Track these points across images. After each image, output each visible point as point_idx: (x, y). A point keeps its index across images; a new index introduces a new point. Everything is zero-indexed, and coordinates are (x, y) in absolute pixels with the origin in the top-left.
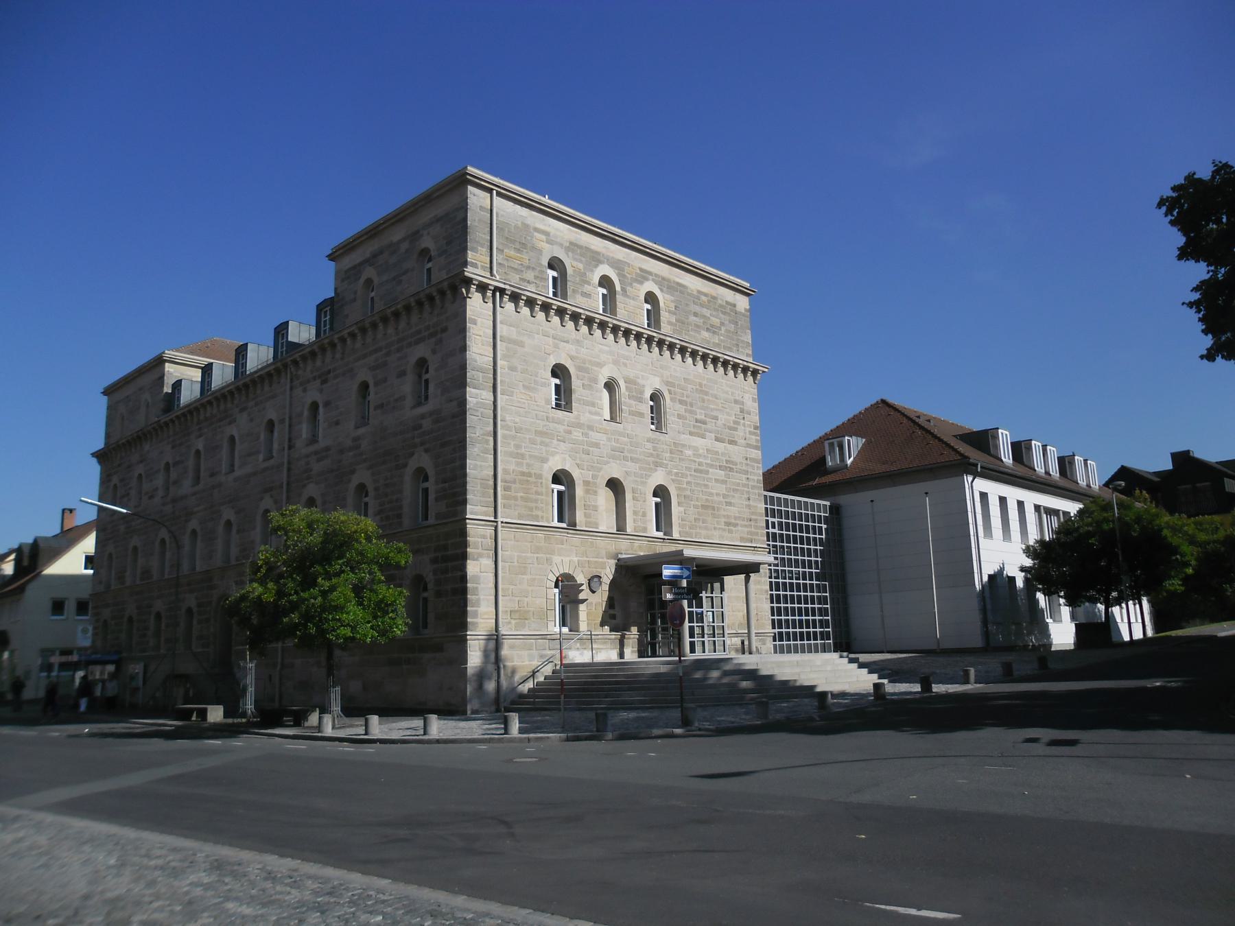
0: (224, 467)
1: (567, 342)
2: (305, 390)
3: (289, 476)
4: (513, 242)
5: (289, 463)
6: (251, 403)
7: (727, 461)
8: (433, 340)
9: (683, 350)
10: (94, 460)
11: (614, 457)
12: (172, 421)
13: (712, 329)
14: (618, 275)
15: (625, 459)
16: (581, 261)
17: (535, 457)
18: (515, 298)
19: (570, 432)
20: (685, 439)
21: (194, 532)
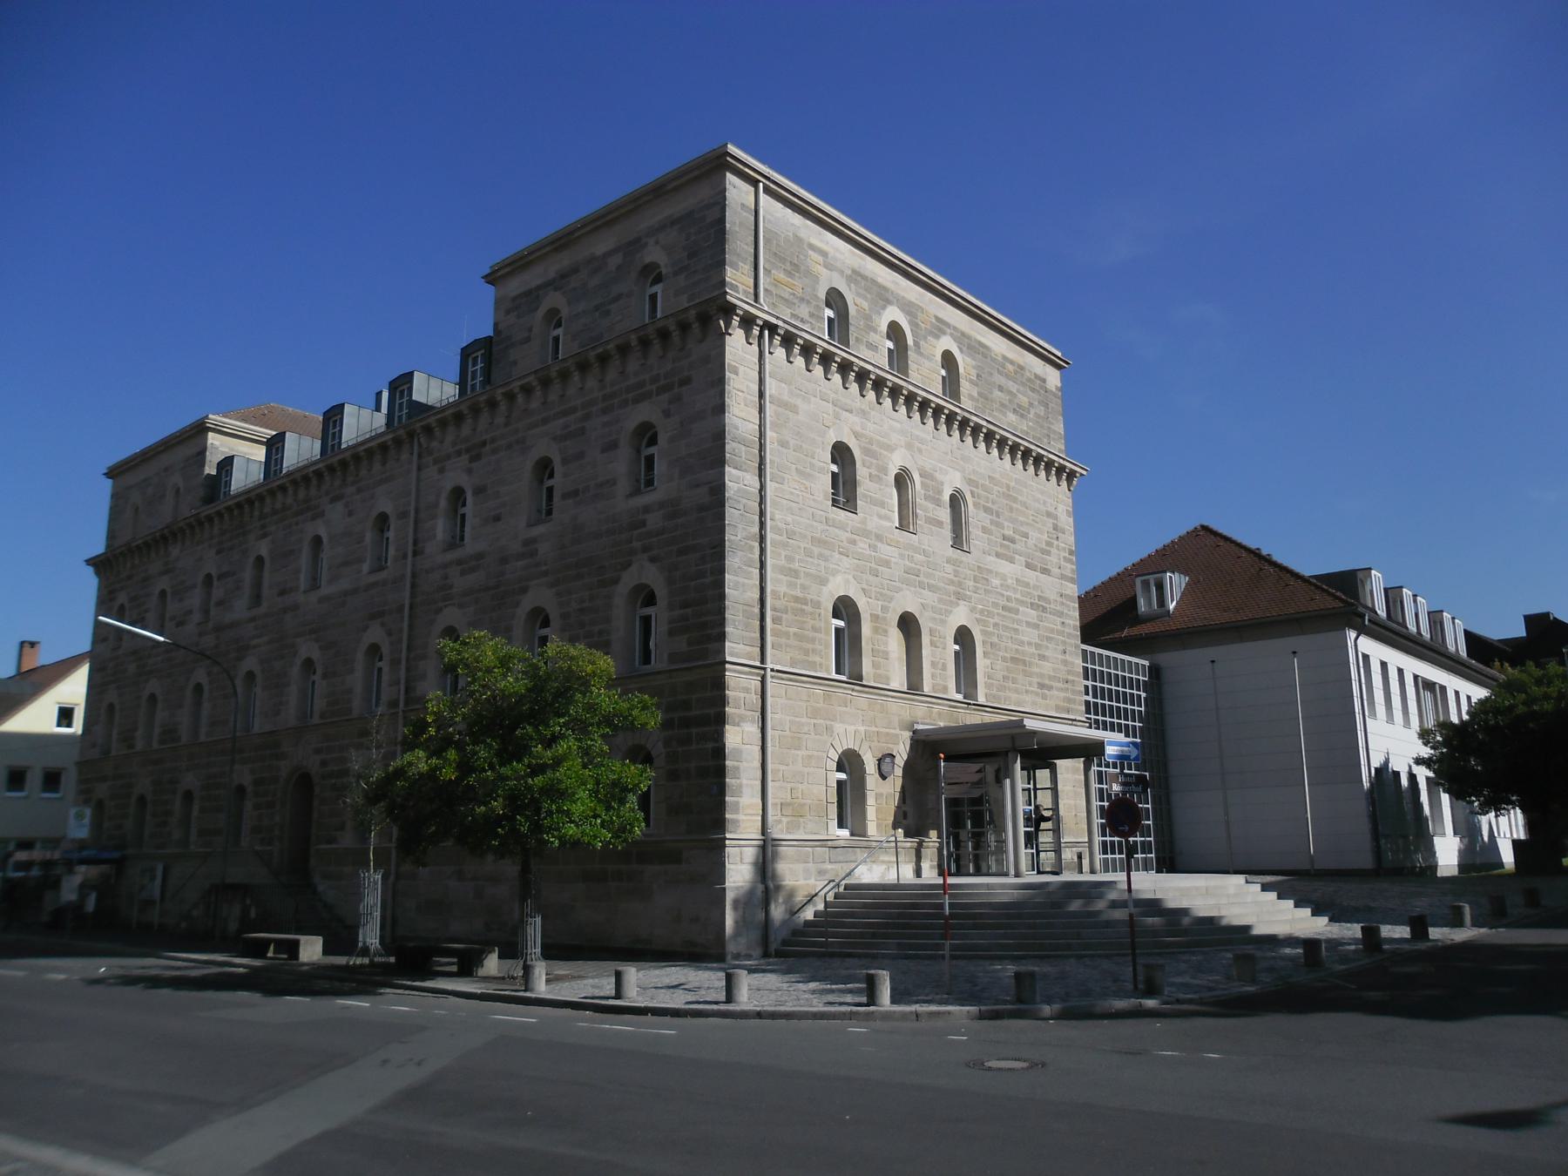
0: (303, 581)
1: (851, 412)
2: (441, 471)
3: (413, 595)
4: (783, 260)
5: (414, 575)
6: (350, 490)
7: (1040, 597)
8: (666, 396)
9: (989, 437)
10: (90, 570)
12: (220, 514)
13: (1019, 411)
14: (911, 323)
15: (921, 585)
16: (865, 298)
18: (788, 341)
19: (854, 542)
20: (992, 562)
21: (250, 675)
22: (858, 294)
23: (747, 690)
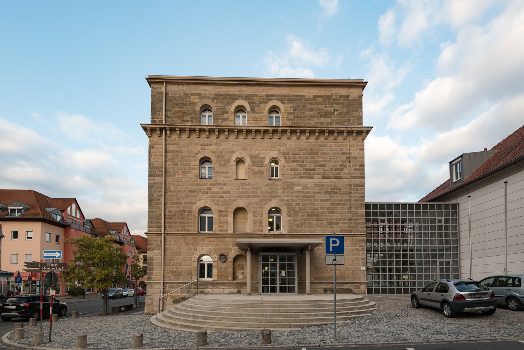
1: (211, 145)
7: (331, 189)
11: (241, 197)
13: (327, 115)
15: (249, 197)
16: (222, 102)
17: (188, 203)
19: (211, 189)
22: (217, 102)
23: (156, 241)
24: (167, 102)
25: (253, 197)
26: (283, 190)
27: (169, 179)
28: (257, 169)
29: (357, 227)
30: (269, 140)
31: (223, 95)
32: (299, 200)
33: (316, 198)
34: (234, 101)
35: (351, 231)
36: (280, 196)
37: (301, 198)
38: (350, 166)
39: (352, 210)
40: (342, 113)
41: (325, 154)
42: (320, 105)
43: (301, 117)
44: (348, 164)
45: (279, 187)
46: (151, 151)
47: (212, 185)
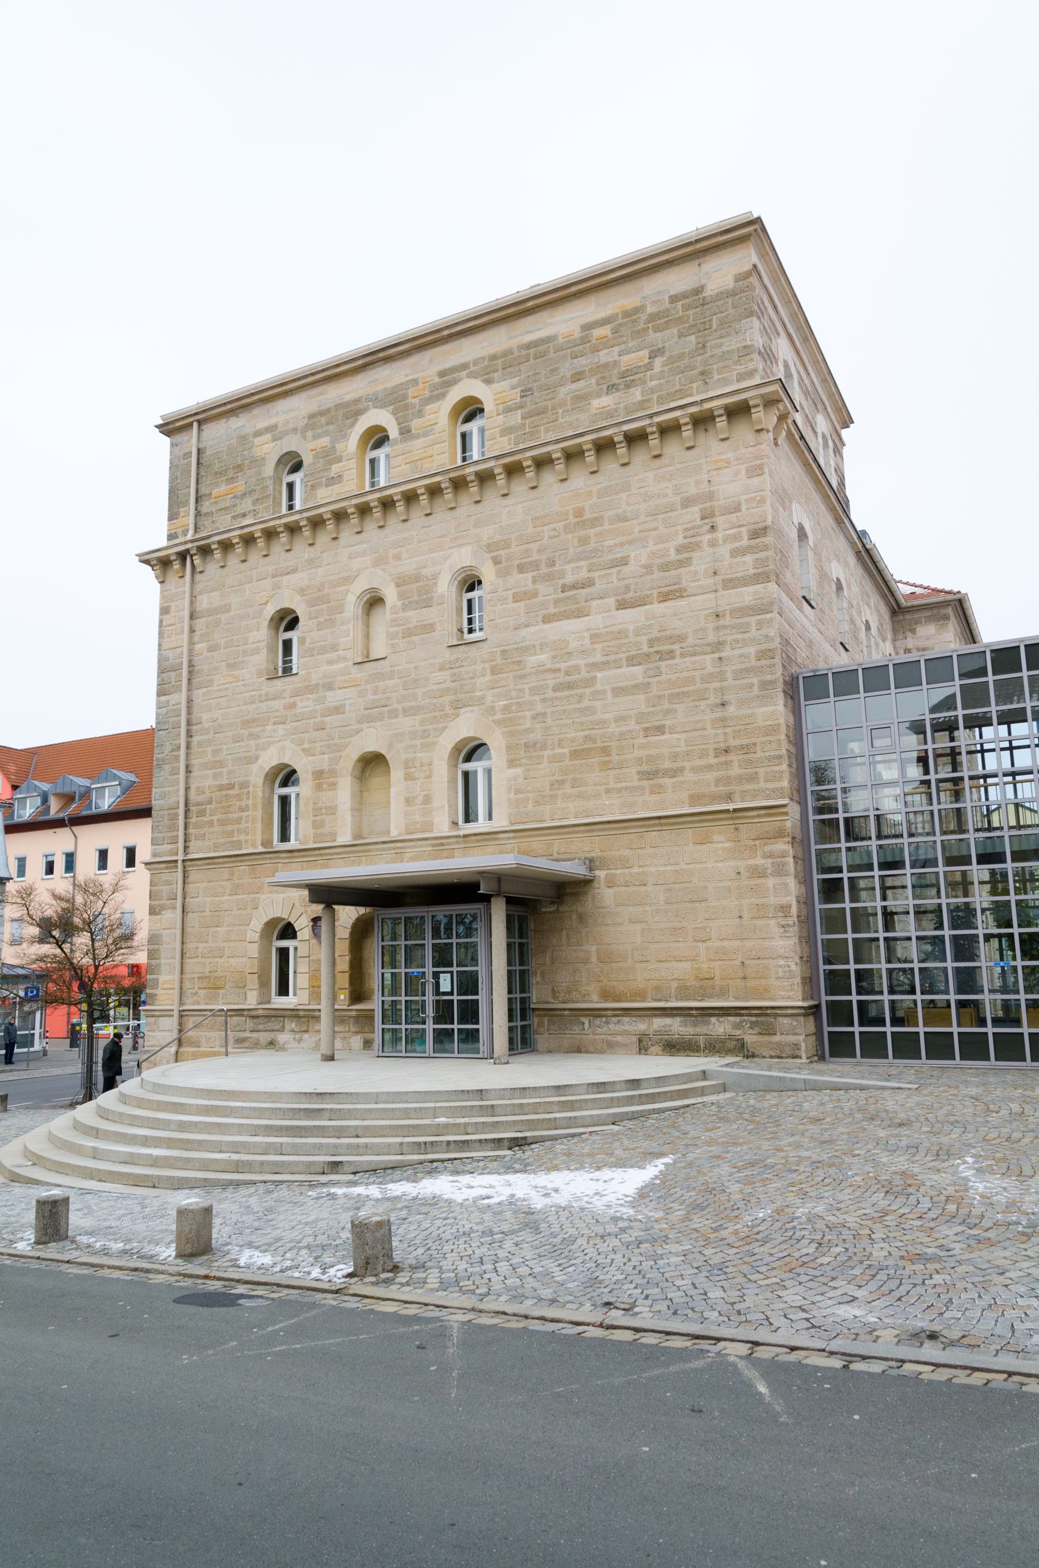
1: (295, 571)
11: (369, 719)
13: (628, 379)
15: (393, 714)
16: (326, 433)
19: (293, 705)
24: (202, 473)
25: (405, 712)
26: (493, 673)
27: (198, 694)
28: (414, 617)
29: (753, 778)
30: (449, 515)
31: (329, 410)
32: (543, 701)
33: (598, 686)
34: (356, 420)
35: (729, 797)
36: (483, 698)
37: (550, 694)
38: (713, 544)
39: (731, 710)
40: (681, 357)
41: (626, 520)
42: (602, 353)
43: (543, 411)
44: (706, 538)
45: (479, 667)
46: (164, 623)
47: (296, 693)
